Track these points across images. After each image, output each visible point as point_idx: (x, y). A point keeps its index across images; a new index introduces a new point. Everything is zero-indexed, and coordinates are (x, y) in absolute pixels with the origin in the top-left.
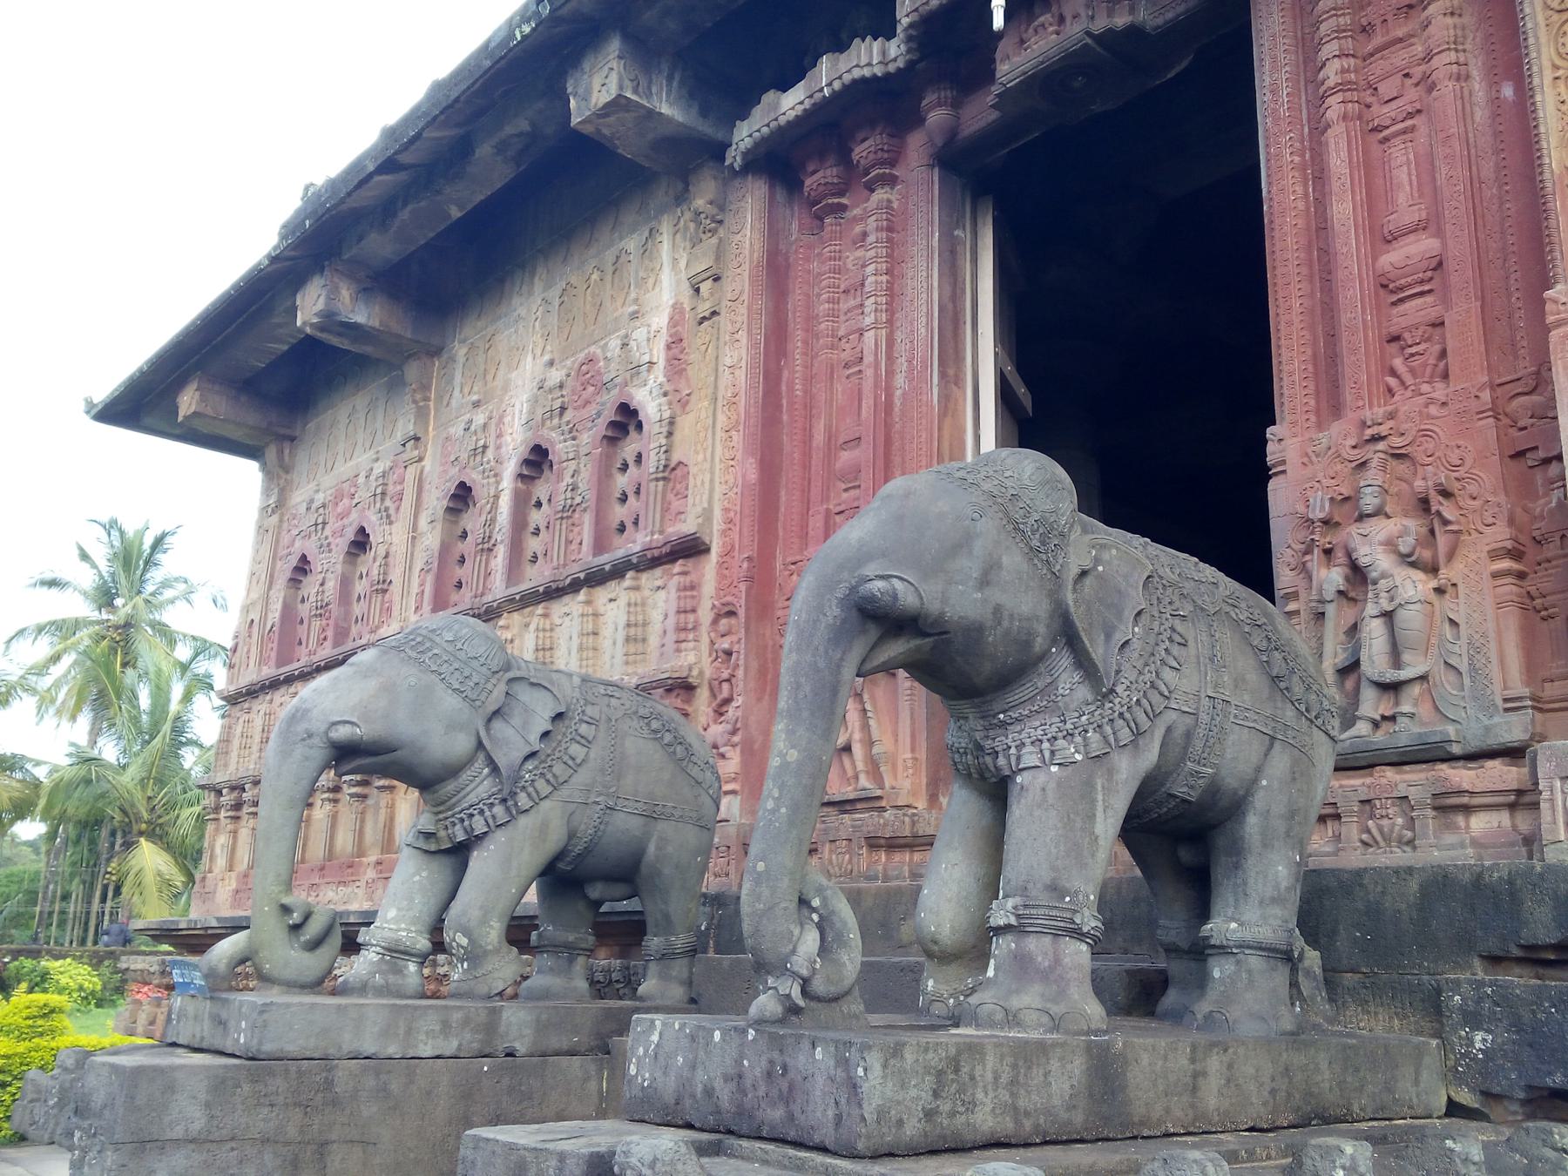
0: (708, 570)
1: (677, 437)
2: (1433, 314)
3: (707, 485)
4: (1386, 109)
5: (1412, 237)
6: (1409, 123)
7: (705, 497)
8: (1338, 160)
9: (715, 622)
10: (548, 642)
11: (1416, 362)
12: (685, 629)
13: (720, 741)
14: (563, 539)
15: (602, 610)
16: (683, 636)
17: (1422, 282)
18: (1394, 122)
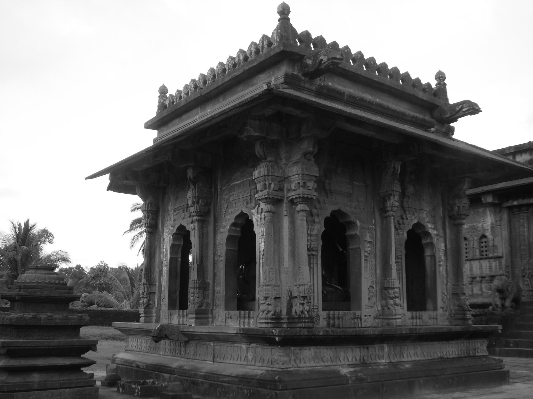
0: (503, 261)
1: (494, 241)
9: (506, 268)
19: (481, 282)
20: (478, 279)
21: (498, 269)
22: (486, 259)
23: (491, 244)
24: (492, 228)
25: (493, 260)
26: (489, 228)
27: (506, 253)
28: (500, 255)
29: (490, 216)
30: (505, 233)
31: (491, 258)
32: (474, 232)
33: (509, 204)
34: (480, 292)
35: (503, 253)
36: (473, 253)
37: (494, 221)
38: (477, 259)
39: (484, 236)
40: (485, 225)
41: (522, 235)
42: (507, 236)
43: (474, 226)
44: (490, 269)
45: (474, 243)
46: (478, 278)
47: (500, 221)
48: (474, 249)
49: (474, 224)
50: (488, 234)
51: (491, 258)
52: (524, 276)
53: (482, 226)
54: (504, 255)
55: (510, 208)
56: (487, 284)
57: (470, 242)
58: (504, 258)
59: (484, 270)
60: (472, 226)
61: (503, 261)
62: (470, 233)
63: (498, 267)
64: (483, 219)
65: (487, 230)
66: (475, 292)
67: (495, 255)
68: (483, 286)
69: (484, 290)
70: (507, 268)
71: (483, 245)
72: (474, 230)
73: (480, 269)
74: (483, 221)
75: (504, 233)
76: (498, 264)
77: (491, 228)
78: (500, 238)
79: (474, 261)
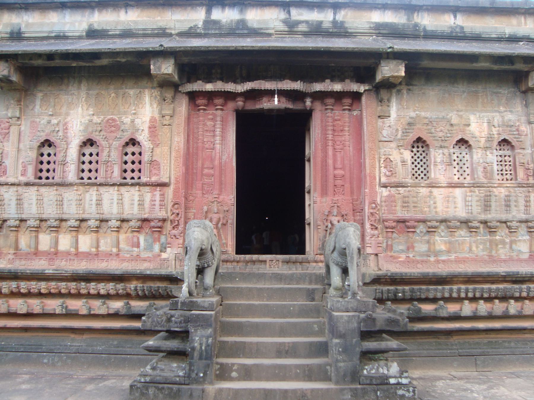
0: (170, 191)
1: (154, 153)
2: (343, 184)
3: (169, 170)
4: (337, 146)
5: (339, 170)
6: (340, 150)
7: (168, 173)
8: (330, 152)
9: (173, 206)
10: (100, 199)
11: (339, 191)
12: (162, 206)
13: (176, 234)
14: (104, 170)
15: (123, 193)
16: (162, 207)
18: (338, 149)
21: (157, 207)
22: (132, 185)
23: (146, 157)
24: (153, 129)
25: (147, 189)
27: (176, 178)
28: (165, 180)
29: (151, 105)
30: (179, 140)
31: (146, 185)
32: (112, 132)
33: (198, 86)
34: (115, 250)
35: (170, 178)
36: (106, 171)
37: (157, 116)
38: (114, 185)
39: (133, 142)
40: (138, 121)
41: (207, 149)
42: (182, 145)
43: (114, 120)
45: (109, 152)
46: (114, 221)
48: (109, 164)
50: (143, 137)
51: (146, 185)
53: (133, 121)
54: (173, 181)
55: (193, 96)
56: (130, 235)
57: (102, 151)
58: (172, 187)
59: (127, 206)
60: (109, 120)
62: (102, 133)
63: (157, 203)
64: (135, 110)
65: (140, 131)
66: (102, 248)
67: (154, 179)
68: (122, 237)
70: (176, 206)
71: (129, 158)
72: (113, 129)
73: (118, 203)
74: (135, 114)
75: (176, 139)
76: (158, 198)
77: (150, 128)
78: (166, 149)
79: (107, 187)
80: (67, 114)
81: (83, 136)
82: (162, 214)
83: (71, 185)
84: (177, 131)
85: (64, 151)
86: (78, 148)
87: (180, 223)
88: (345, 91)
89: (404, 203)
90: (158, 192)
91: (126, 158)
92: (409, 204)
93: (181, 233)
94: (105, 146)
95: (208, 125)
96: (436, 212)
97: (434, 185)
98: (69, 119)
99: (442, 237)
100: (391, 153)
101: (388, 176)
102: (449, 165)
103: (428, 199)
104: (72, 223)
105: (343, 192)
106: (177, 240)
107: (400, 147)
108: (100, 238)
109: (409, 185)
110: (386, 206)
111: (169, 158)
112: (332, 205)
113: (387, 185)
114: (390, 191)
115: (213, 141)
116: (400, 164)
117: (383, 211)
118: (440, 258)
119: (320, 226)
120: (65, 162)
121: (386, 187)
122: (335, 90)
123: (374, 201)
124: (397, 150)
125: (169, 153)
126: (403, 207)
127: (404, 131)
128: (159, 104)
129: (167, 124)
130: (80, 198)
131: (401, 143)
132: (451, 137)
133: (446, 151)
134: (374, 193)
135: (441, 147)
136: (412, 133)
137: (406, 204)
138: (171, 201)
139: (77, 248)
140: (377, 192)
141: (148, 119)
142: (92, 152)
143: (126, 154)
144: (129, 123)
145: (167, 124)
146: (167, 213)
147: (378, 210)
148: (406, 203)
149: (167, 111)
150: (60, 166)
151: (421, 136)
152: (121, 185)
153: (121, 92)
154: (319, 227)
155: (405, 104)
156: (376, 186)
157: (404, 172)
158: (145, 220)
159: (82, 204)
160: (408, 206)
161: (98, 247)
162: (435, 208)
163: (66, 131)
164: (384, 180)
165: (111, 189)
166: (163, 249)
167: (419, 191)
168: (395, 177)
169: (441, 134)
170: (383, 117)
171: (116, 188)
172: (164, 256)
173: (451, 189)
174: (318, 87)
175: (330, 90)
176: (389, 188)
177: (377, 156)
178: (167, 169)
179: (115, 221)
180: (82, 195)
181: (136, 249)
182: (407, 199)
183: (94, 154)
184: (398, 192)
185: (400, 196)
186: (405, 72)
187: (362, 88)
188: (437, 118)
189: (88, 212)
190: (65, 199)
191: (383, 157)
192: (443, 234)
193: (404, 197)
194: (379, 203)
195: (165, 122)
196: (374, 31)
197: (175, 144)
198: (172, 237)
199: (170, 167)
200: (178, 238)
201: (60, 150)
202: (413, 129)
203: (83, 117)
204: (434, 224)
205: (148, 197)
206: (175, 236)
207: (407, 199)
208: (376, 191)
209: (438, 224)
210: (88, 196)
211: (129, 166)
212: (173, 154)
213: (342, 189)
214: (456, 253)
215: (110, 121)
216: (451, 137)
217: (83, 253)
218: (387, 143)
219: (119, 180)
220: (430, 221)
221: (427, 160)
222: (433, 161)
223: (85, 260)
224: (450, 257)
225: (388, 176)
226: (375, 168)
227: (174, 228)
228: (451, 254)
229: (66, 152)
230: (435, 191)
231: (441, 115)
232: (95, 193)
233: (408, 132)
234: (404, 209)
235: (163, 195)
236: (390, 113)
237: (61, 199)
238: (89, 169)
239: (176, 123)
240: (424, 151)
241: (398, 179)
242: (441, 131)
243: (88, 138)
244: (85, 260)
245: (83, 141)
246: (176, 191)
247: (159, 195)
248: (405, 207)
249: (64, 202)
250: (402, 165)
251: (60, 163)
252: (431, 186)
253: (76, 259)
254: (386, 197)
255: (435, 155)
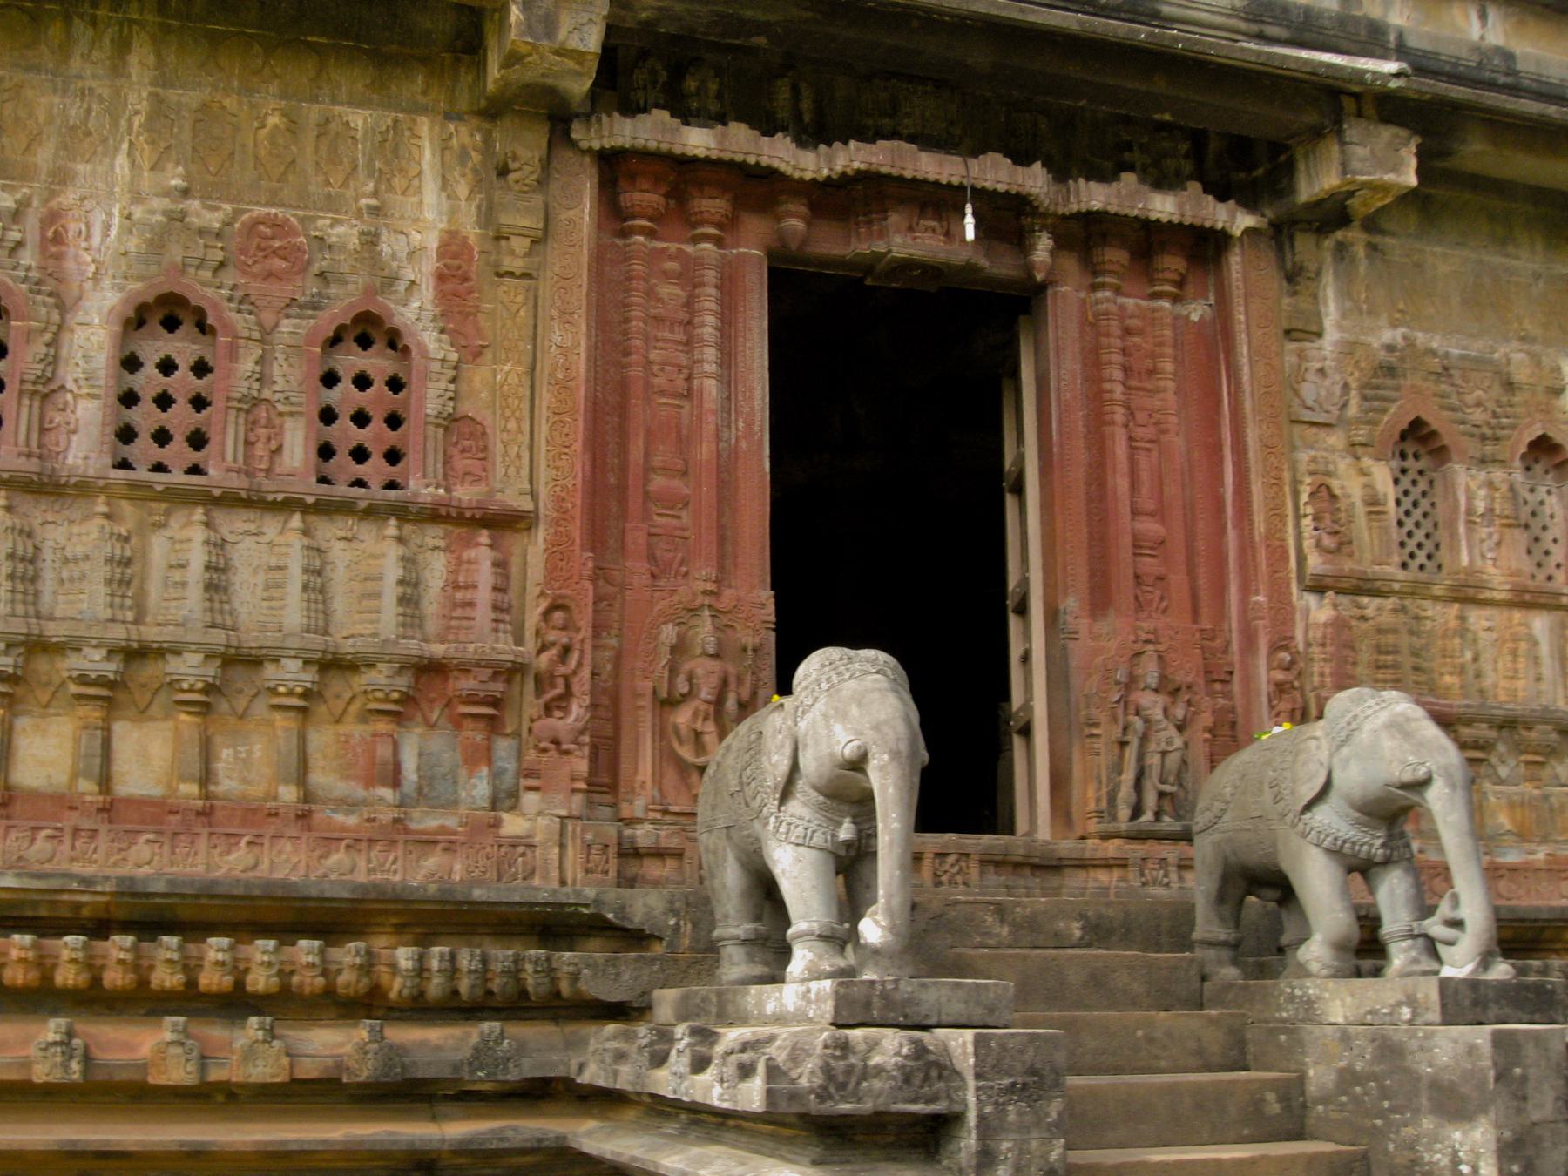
0: (533, 551)
2: (1161, 571)
3: (526, 460)
7: (525, 472)
8: (1120, 450)
9: (546, 615)
10: (222, 561)
11: (1149, 597)
12: (502, 610)
13: (563, 735)
15: (324, 546)
16: (501, 616)
17: (1152, 548)
18: (1142, 440)
19: (306, 706)
20: (291, 673)
21: (483, 614)
22: (373, 513)
23: (430, 399)
25: (433, 535)
26: (429, 265)
27: (560, 500)
28: (514, 498)
31: (435, 515)
32: (270, 275)
34: (288, 794)
35: (534, 495)
36: (247, 443)
37: (471, 230)
38: (289, 505)
41: (662, 393)
43: (278, 226)
44: (403, 600)
45: (260, 361)
46: (293, 665)
47: (539, 241)
48: (262, 413)
49: (292, 216)
51: (435, 515)
52: (670, 703)
53: (371, 240)
54: (546, 508)
56: (357, 731)
57: (233, 353)
58: (541, 534)
60: (257, 222)
61: (533, 551)
62: (229, 277)
64: (375, 194)
65: (401, 287)
66: (227, 783)
67: (465, 494)
68: (321, 739)
69: (323, 778)
70: (558, 616)
71: (344, 396)
72: (278, 264)
73: (305, 588)
74: (375, 211)
75: (557, 336)
76: (485, 575)
77: (441, 278)
78: (510, 372)
80: (62, 177)
81: (140, 278)
82: (504, 649)
83: (83, 489)
84: (558, 303)
85: (48, 337)
86: (117, 328)
87: (576, 688)
88: (1187, 222)
89: (1380, 652)
90: (481, 554)
91: (334, 396)
92: (1400, 659)
93: (582, 732)
94: (246, 333)
95: (666, 298)
96: (1481, 691)
97: (1471, 592)
98: (69, 197)
99: (1501, 782)
100: (1331, 467)
101: (1329, 552)
102: (1509, 526)
103: (1457, 641)
104: (94, 661)
105: (1164, 604)
106: (565, 759)
107: (1360, 450)
108: (218, 740)
109: (1396, 586)
110: (1325, 660)
111: (526, 413)
112: (1138, 647)
113: (1329, 581)
114: (1335, 606)
115: (684, 363)
116: (1360, 510)
117: (1316, 679)
118: (1500, 860)
119: (1096, 725)
120: (53, 386)
121: (1318, 588)
122: (1153, 216)
123: (1285, 638)
124: (1349, 460)
125: (528, 393)
126: (1379, 667)
127: (1369, 393)
128: (477, 185)
129: (518, 272)
130: (128, 553)
131: (1362, 434)
132: (1513, 427)
133: (1498, 475)
134: (1282, 612)
135: (1483, 461)
136: (1393, 401)
137: (1390, 658)
138: (537, 591)
139: (105, 781)
140: (1293, 608)
141: (432, 241)
142: (174, 356)
143: (330, 379)
144: (354, 242)
145: (518, 272)
146: (519, 641)
147: (1300, 674)
148: (1388, 653)
149: (521, 218)
150: (26, 402)
151: (1424, 417)
152: (325, 508)
153: (313, 113)
154: (1095, 731)
155: (1363, 296)
156: (1288, 585)
157: (1376, 542)
158: (430, 670)
159: (135, 583)
160: (1395, 666)
161: (206, 777)
162: (1478, 675)
163: (53, 249)
164: (1314, 562)
165: (271, 526)
166: (503, 799)
167: (1423, 614)
168: (1351, 555)
169: (1478, 416)
170: (1301, 335)
171: (296, 521)
172: (513, 825)
173: (1517, 615)
174: (1094, 196)
175: (1136, 212)
176: (1330, 594)
177: (1287, 476)
178: (519, 456)
179: (300, 663)
180: (134, 541)
181: (387, 793)
182: (1391, 639)
183: (184, 363)
184: (1358, 612)
185: (1364, 626)
186: (1419, 172)
187: (1244, 221)
188: (1463, 357)
189: (160, 619)
190: (47, 554)
191: (1308, 480)
192: (1503, 771)
193: (1379, 631)
194: (1301, 647)
195: (508, 263)
196: (1243, 25)
197: (550, 357)
198: (543, 745)
199: (531, 448)
200: (567, 752)
201: (29, 332)
202: (1397, 388)
203: (137, 197)
204: (1483, 731)
205: (436, 570)
206: (556, 742)
207: (1391, 639)
208: (1290, 603)
209: (1493, 734)
210: (158, 546)
211: (345, 433)
212: (545, 398)
213: (1158, 593)
214: (1545, 840)
215: (262, 228)
216: (1513, 427)
217: (130, 801)
218: (1314, 430)
219: (310, 490)
220: (1469, 722)
221: (1433, 504)
222: (1463, 508)
223: (151, 836)
224: (1531, 857)
225: (1329, 552)
226: (1282, 517)
227: (548, 709)
228: (1533, 847)
229: (54, 343)
230: (1478, 618)
231: (1476, 348)
232: (198, 534)
233: (1385, 399)
234: (1380, 676)
235: (501, 565)
236: (1321, 325)
237: (30, 550)
238: (156, 426)
239: (557, 270)
240: (1421, 472)
241: (1360, 562)
242: (1479, 404)
243: (166, 289)
244: (151, 836)
245: (140, 300)
246: (557, 553)
247: (488, 563)
248: (1386, 667)
249: (40, 564)
250: (1370, 513)
251: (29, 387)
252: (1462, 595)
253: (103, 829)
254: (1325, 625)
255: (1468, 489)
